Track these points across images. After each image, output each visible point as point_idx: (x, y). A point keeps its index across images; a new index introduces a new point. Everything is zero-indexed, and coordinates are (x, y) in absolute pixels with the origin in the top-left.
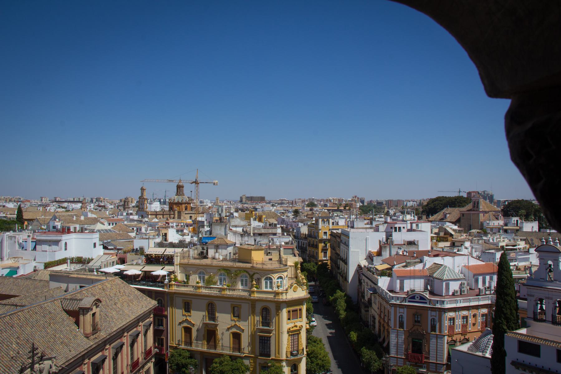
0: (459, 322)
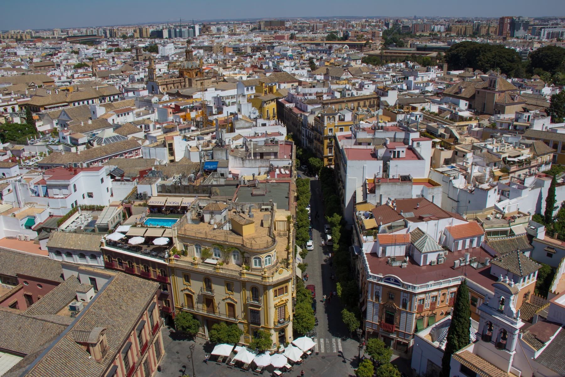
0: (428, 302)
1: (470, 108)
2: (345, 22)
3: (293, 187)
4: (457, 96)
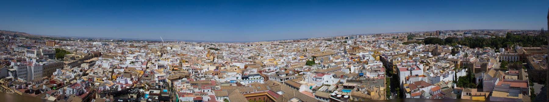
1: (432, 54)
2: (397, 34)
3: (385, 80)
4: (428, 51)
